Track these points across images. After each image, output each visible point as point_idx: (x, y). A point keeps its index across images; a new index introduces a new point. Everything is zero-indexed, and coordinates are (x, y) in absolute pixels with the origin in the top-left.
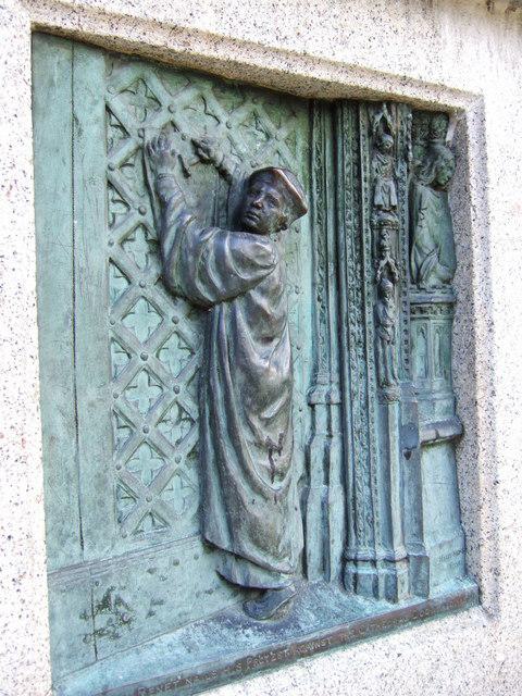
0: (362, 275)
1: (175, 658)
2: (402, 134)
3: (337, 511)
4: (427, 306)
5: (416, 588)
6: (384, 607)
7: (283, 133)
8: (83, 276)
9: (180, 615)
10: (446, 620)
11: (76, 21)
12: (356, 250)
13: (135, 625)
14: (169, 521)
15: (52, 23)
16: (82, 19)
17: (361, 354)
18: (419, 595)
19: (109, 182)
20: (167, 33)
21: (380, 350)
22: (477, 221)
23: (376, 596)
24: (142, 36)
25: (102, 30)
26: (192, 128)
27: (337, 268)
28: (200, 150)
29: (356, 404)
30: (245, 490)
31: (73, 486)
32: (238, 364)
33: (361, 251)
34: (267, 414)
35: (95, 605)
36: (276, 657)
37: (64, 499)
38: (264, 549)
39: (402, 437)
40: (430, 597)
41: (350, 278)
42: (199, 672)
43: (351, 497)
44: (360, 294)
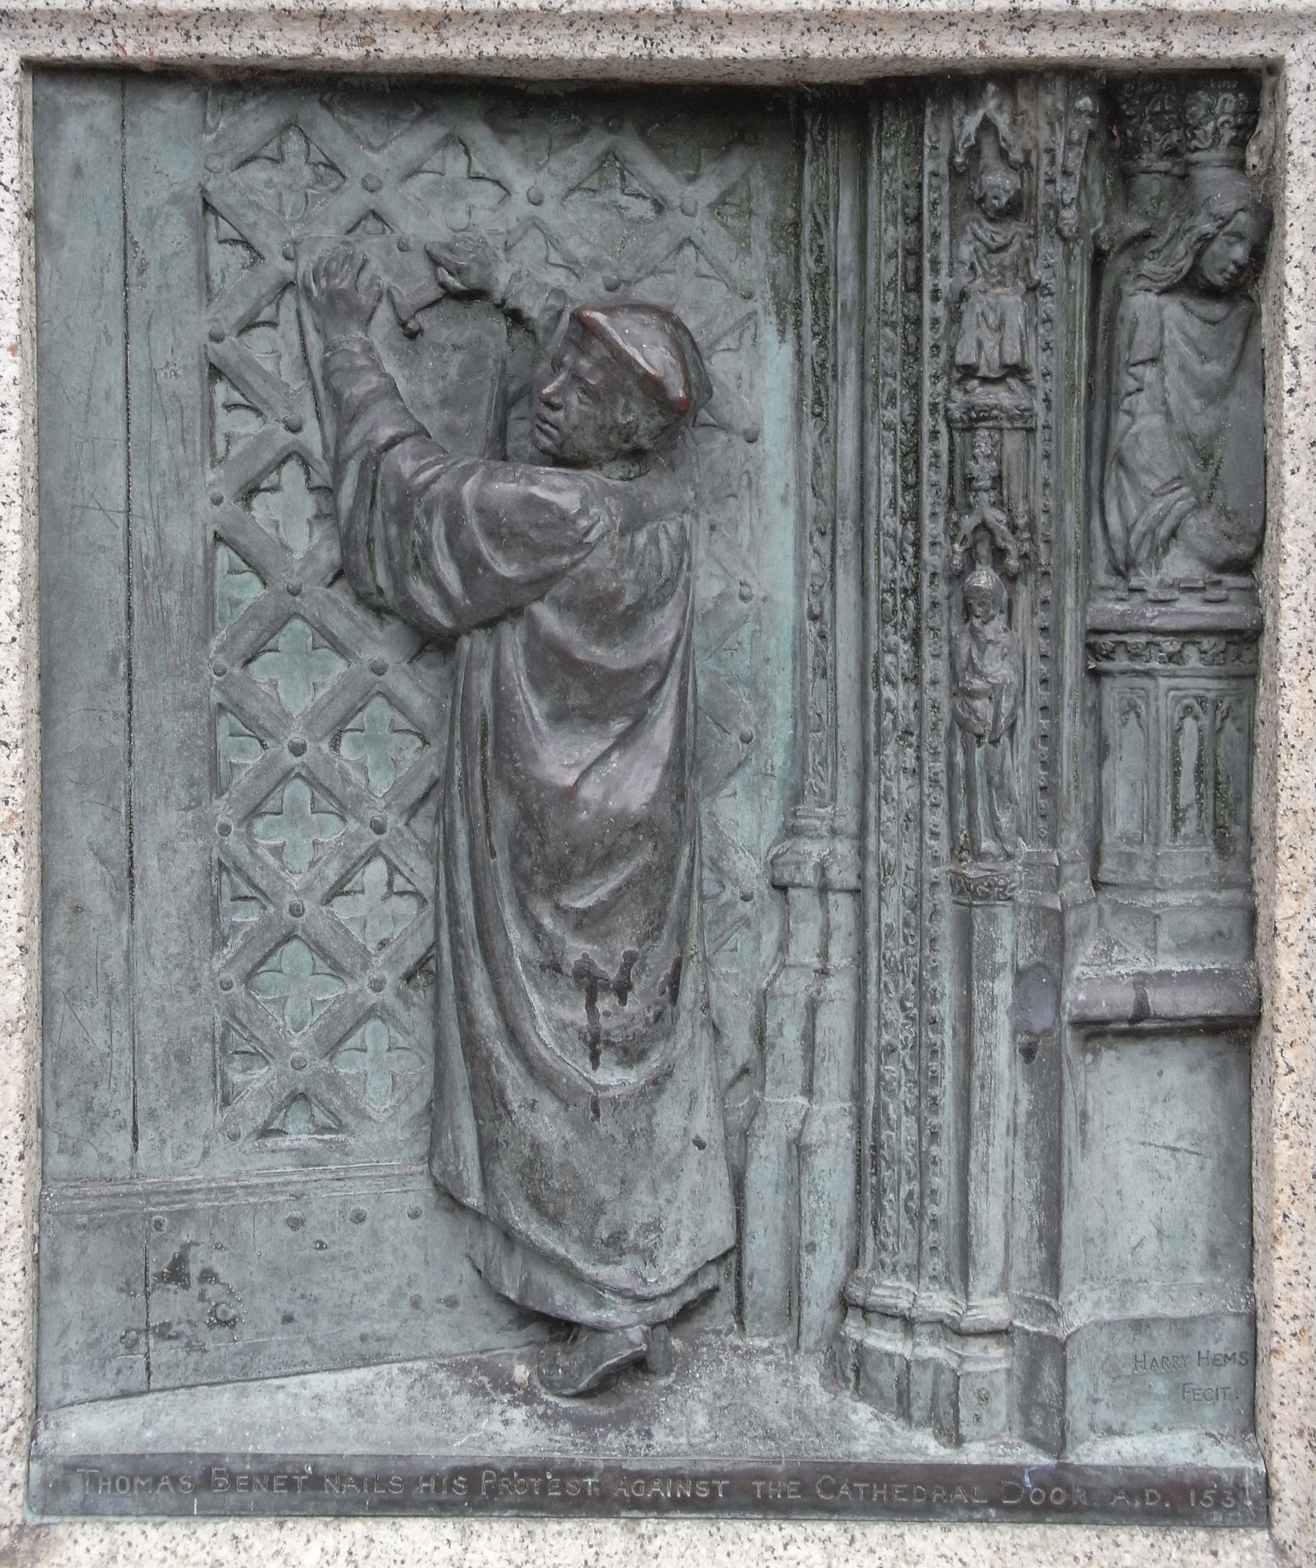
0: (917, 556)
1: (314, 1424)
2: (1052, 162)
3: (832, 1172)
4: (1142, 639)
5: (1028, 1422)
6: (926, 1447)
7: (707, 190)
8: (149, 572)
9: (363, 1338)
10: (1123, 1537)
11: (108, 39)
12: (906, 487)
13: (246, 1335)
14: (347, 1118)
15: (60, 53)
16: (119, 32)
17: (910, 763)
18: (1036, 1442)
19: (212, 366)
20: (313, 27)
21: (959, 758)
22: (1300, 393)
23: (904, 1412)
24: (258, 43)
25: (171, 47)
26: (425, 218)
27: (862, 533)
28: (441, 271)
29: (894, 896)
30: (511, 1072)
31: (119, 1014)
32: (499, 776)
33: (913, 488)
34: (582, 900)
35: (152, 1270)
36: (563, 1487)
37: (100, 1036)
38: (555, 1221)
39: (1020, 1005)
40: (1072, 1459)
41: (886, 561)
42: (359, 1469)
43: (868, 1141)
44: (911, 603)
